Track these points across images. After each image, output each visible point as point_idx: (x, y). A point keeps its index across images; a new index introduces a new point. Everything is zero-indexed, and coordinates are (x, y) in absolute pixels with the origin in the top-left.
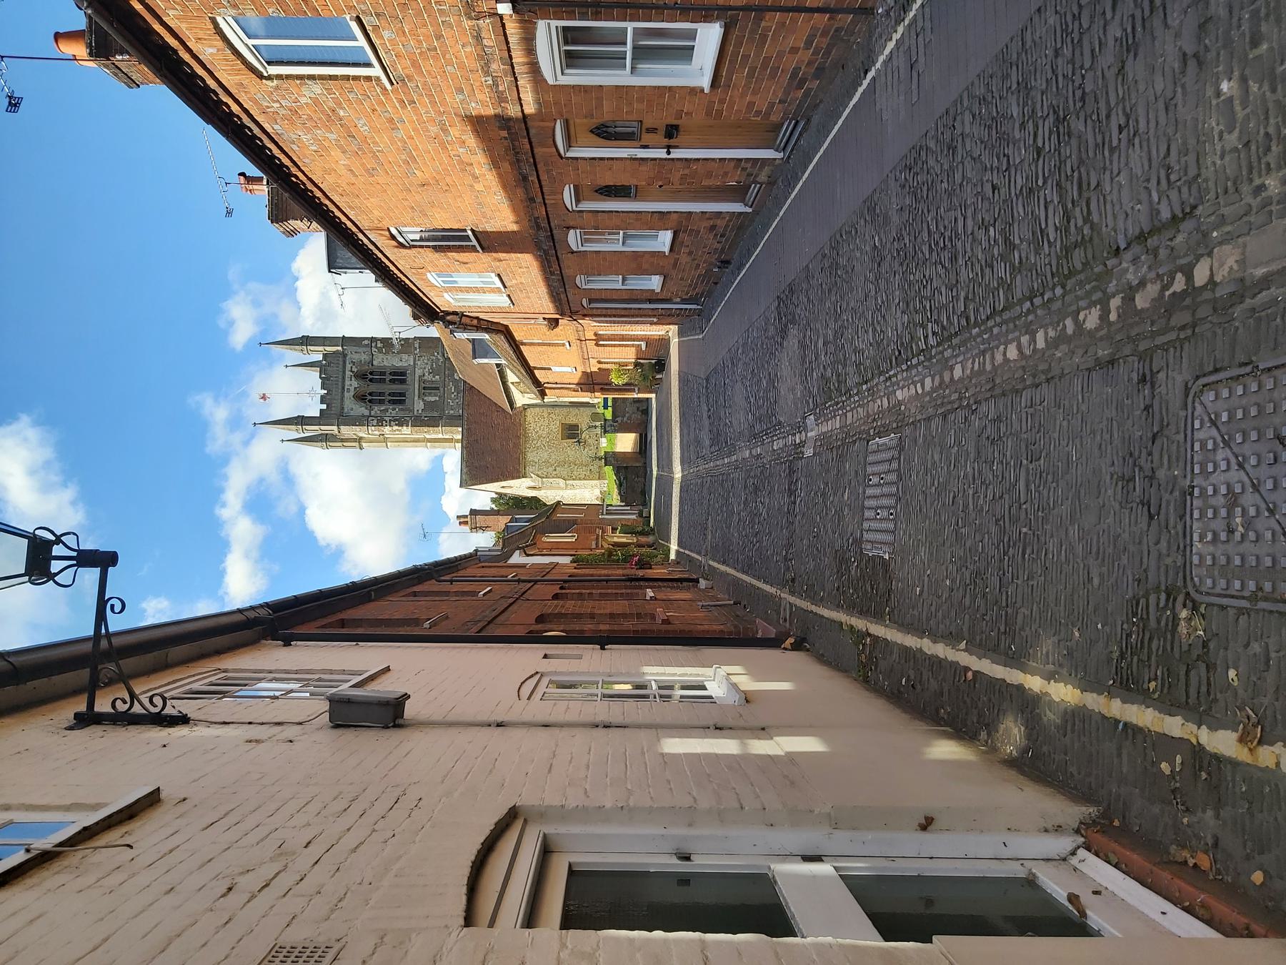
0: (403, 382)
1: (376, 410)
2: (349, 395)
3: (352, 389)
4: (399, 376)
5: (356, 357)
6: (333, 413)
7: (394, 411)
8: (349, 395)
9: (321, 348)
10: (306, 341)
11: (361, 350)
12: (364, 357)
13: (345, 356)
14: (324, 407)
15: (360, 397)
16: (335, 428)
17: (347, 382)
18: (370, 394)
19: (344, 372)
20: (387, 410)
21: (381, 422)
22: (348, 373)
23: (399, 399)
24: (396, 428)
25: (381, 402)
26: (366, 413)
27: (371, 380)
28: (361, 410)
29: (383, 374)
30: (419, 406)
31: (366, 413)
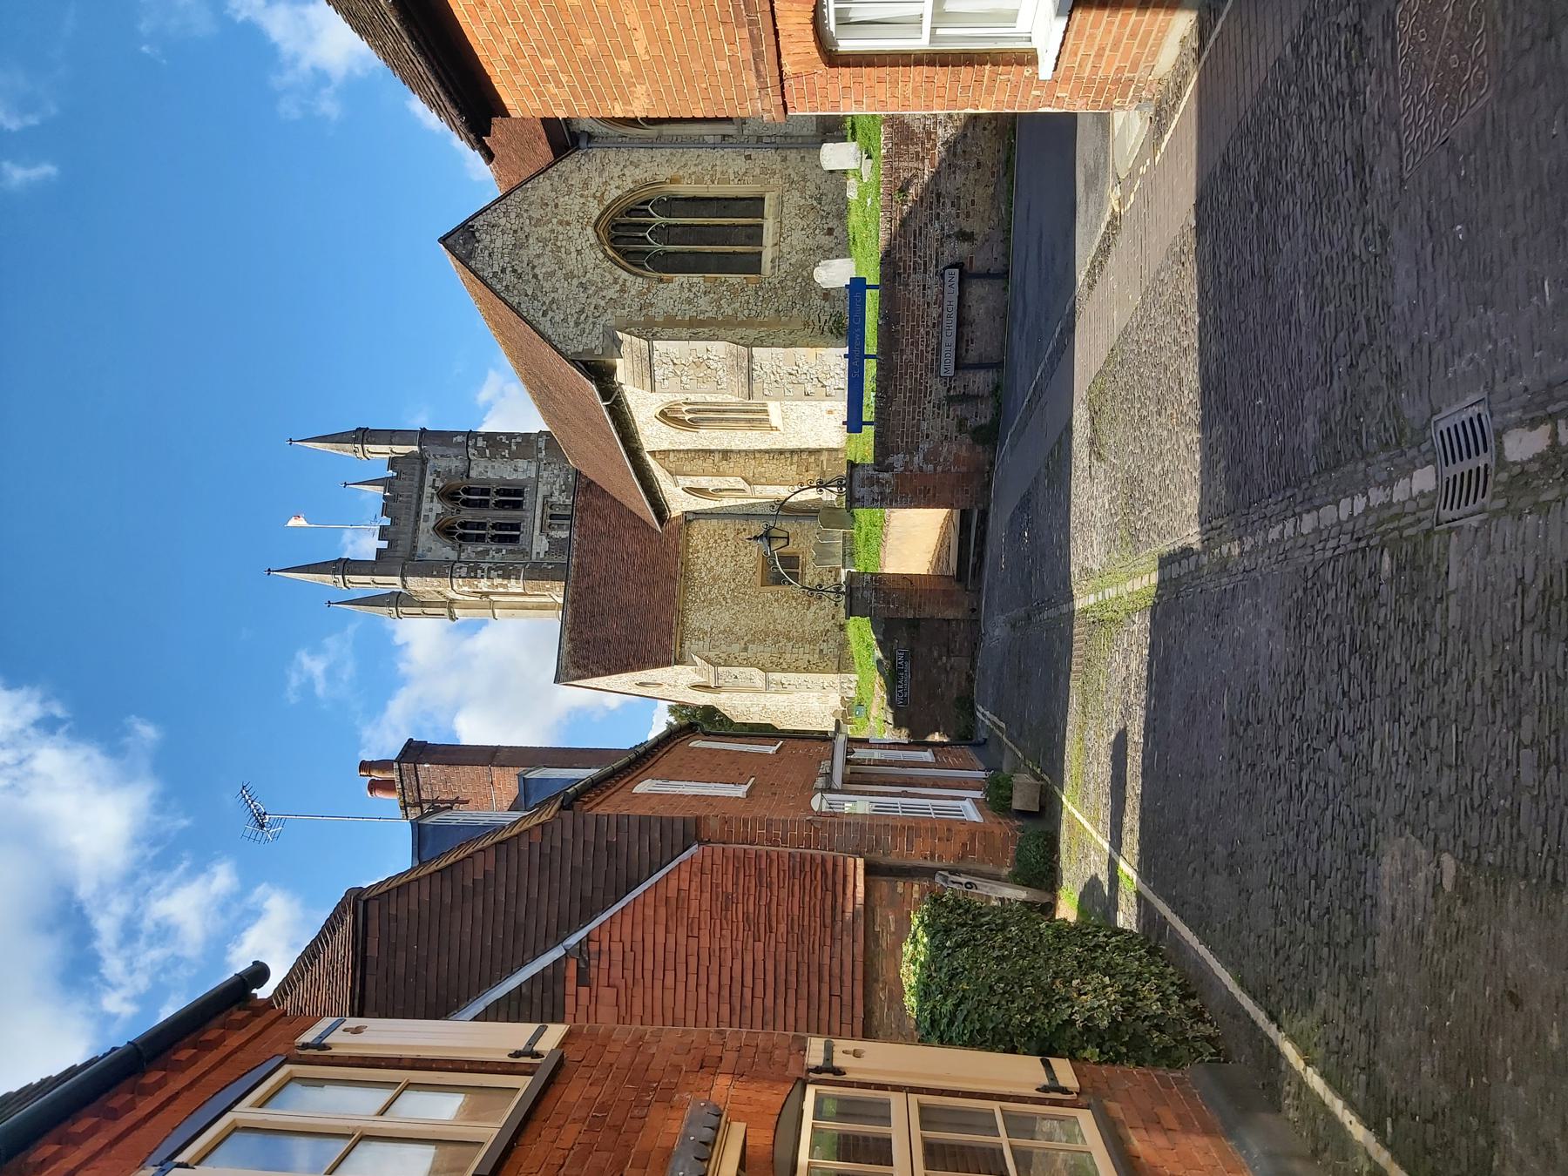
0: (518, 505)
1: (470, 550)
2: (426, 526)
3: (432, 516)
4: (512, 497)
5: (443, 464)
6: (397, 556)
7: (498, 553)
8: (426, 526)
9: (385, 448)
10: (363, 436)
11: (450, 452)
12: (456, 464)
13: (424, 462)
14: (384, 545)
15: (445, 530)
16: (397, 580)
17: (426, 505)
18: (464, 525)
19: (421, 488)
21: (473, 572)
22: (428, 490)
23: (508, 535)
24: (497, 581)
25: (480, 538)
26: (453, 555)
27: (466, 503)
28: (445, 551)
29: (486, 492)
30: (540, 545)
31: (453, 555)
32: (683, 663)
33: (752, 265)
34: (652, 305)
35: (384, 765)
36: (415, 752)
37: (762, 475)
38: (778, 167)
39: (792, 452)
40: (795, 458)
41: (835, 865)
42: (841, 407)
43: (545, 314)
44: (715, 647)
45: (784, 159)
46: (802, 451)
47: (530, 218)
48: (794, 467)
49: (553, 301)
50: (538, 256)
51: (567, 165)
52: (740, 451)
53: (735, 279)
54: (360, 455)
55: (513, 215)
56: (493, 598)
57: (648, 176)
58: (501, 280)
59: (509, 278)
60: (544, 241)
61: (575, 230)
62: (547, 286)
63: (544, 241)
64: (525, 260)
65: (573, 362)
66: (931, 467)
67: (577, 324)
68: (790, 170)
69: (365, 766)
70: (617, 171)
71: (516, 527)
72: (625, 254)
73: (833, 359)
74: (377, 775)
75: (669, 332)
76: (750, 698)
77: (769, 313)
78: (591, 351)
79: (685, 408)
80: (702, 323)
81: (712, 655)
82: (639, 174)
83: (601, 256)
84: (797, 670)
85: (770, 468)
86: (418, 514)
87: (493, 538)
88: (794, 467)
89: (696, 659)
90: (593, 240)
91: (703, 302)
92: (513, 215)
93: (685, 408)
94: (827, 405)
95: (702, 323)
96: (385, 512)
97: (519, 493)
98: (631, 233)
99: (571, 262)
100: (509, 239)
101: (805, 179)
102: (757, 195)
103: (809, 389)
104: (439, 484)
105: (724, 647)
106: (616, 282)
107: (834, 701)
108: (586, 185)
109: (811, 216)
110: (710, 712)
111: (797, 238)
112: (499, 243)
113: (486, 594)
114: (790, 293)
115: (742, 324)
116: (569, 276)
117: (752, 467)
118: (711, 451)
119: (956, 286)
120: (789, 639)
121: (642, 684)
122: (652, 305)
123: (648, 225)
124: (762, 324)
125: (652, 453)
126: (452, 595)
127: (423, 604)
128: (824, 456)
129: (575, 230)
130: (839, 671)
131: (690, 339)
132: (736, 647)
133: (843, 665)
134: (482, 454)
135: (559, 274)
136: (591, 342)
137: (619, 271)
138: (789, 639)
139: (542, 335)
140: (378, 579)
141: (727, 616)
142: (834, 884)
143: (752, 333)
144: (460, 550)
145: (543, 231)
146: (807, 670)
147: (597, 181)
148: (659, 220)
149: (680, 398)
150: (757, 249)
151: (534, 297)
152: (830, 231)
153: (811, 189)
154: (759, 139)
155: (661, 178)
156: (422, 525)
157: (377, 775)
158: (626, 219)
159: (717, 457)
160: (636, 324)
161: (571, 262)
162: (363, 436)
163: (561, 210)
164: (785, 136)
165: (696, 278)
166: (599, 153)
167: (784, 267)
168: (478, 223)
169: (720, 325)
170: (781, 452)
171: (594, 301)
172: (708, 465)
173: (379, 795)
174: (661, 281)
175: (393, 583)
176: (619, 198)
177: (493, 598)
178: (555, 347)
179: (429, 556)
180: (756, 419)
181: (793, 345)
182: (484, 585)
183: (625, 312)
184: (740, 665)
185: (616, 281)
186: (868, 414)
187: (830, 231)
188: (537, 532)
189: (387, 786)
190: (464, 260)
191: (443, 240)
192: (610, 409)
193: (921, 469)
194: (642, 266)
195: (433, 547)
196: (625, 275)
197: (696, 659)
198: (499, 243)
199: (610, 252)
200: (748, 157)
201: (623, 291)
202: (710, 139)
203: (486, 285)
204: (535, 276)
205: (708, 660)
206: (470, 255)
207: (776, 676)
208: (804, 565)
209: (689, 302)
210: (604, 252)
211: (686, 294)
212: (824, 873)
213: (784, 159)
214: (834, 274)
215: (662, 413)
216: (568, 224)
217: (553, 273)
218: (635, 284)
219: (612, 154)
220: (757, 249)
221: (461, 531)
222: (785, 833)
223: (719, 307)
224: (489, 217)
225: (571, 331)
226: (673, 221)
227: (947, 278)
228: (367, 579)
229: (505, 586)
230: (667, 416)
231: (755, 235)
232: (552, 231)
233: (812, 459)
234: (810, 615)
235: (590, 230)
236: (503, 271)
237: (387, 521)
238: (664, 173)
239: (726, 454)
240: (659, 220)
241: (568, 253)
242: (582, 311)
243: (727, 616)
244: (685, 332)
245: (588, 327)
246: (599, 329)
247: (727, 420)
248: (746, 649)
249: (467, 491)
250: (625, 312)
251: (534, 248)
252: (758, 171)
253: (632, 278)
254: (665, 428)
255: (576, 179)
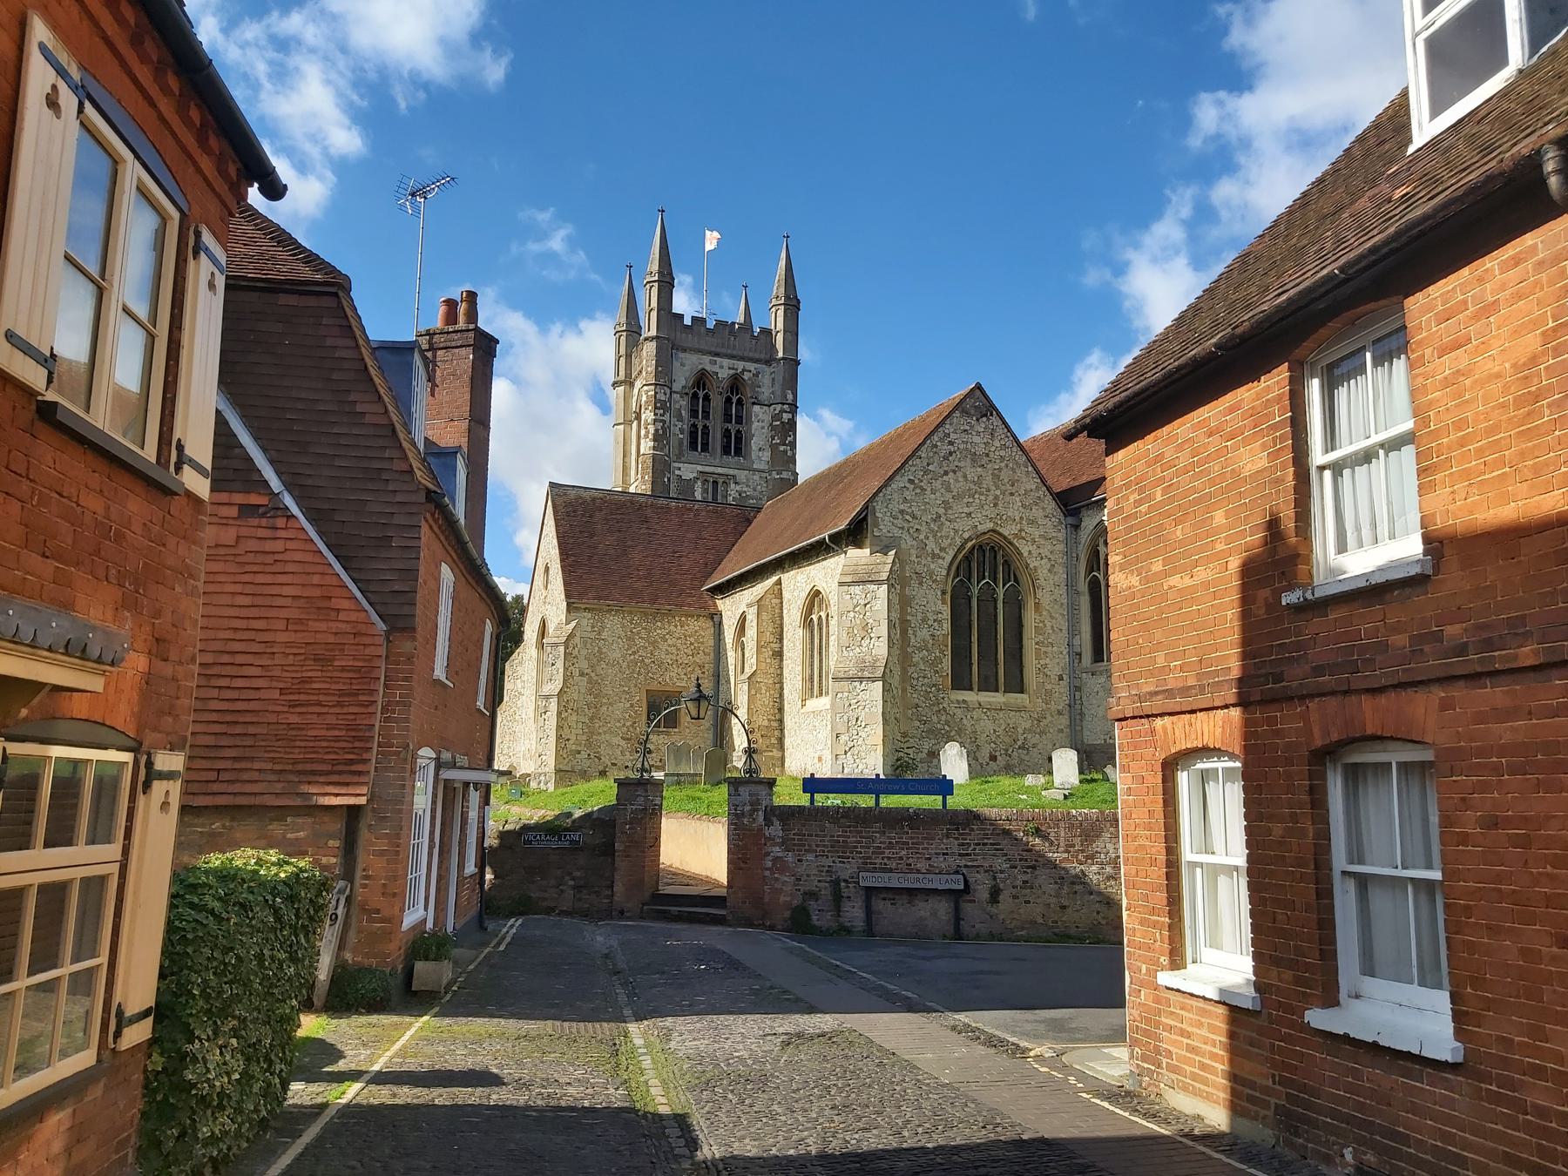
0: (726, 450)
1: (683, 403)
2: (705, 362)
3: (716, 369)
4: (735, 445)
5: (765, 380)
6: (676, 335)
7: (679, 430)
8: (705, 362)
9: (780, 326)
10: (792, 306)
11: (777, 387)
12: (765, 392)
13: (768, 362)
14: (687, 321)
15: (702, 380)
16: (653, 332)
17: (726, 362)
18: (707, 398)
19: (742, 359)
20: (680, 419)
21: (660, 406)
22: (740, 365)
23: (697, 441)
24: (652, 429)
25: (694, 413)
27: (728, 400)
28: (682, 379)
29: (739, 420)
30: (687, 471)
31: (677, 387)
32: (568, 611)
33: (960, 681)
34: (921, 584)
35: (472, 315)
36: (485, 347)
37: (758, 691)
38: (1053, 707)
39: (781, 721)
40: (775, 724)
41: (360, 773)
42: (825, 771)
43: (911, 481)
44: (585, 643)
45: (1060, 713)
46: (782, 730)
47: (1000, 469)
48: (766, 723)
49: (923, 490)
50: (965, 476)
51: (1050, 505)
52: (781, 668)
53: (947, 664)
54: (774, 302)
55: (1003, 453)
56: (635, 424)
57: (1042, 582)
58: (941, 440)
59: (945, 448)
60: (978, 483)
61: (989, 511)
62: (937, 484)
63: (978, 483)
64: (962, 464)
65: (866, 507)
66: (769, 864)
67: (902, 512)
68: (1049, 718)
69: (472, 297)
70: (1045, 552)
71: (705, 448)
72: (967, 558)
73: (871, 763)
74: (462, 309)
75: (896, 600)
76: (530, 682)
77: (915, 698)
78: (876, 525)
79: (823, 614)
80: (904, 632)
81: (577, 640)
82: (1043, 573)
83: (966, 536)
84: (559, 727)
85: (765, 699)
86: (717, 355)
87: (694, 426)
88: (766, 723)
89: (573, 624)
90: (981, 528)
91: (924, 633)
92: (1003, 453)
93: (823, 614)
94: (827, 756)
95: (904, 632)
96: (719, 323)
97: (738, 452)
98: (986, 569)
99: (960, 508)
100: (980, 450)
101: (1042, 733)
102: (1026, 686)
103: (843, 738)
104: (746, 376)
105: (584, 652)
106: (942, 549)
107: (525, 767)
108: (1032, 522)
109: (1007, 739)
110: (517, 639)
111: (986, 726)
112: (977, 439)
113: (638, 417)
114: (935, 718)
115: (904, 671)
116: (947, 505)
117: (766, 680)
118: (781, 640)
119: (947, 886)
120: (591, 719)
121: (547, 569)
122: (921, 584)
123: (995, 580)
124: (904, 690)
125: (779, 582)
126: (638, 384)
127: (629, 356)
128: (776, 754)
129: (989, 511)
130: (558, 771)
131: (890, 621)
132: (584, 665)
133: (565, 775)
134: (776, 417)
135: (948, 496)
136: (884, 523)
137: (952, 553)
138: (591, 719)
139: (891, 478)
140: (654, 314)
141: (617, 655)
142: (340, 773)
143: (895, 681)
144: (683, 394)
145: (988, 481)
146: (559, 737)
147: (1036, 532)
148: (1001, 592)
149: (833, 610)
150: (975, 687)
151: (926, 472)
152: (993, 758)
153: (1035, 739)
154: (1078, 689)
155: (1039, 594)
156: (707, 358)
157: (462, 309)
158: (1000, 560)
159: (776, 646)
160: (902, 567)
161: (960, 508)
162: (792, 306)
163: (1008, 498)
164: (1082, 714)
165: (947, 626)
166: (1061, 535)
167: (958, 712)
168: (994, 419)
169: (903, 650)
170: (781, 710)
171: (923, 528)
172: (768, 637)
173: (442, 310)
174: (944, 593)
175: (650, 327)
176: (1020, 554)
177: (635, 424)
178: (879, 490)
179: (676, 364)
180: (814, 686)
181: (885, 721)
182: (648, 415)
183: (913, 558)
184: (566, 669)
185: (942, 549)
186: (820, 799)
187: (993, 758)
188: (700, 468)
189: (451, 317)
190: (960, 406)
191: (979, 387)
192: (821, 543)
193: (768, 854)
194: (957, 575)
195: (686, 367)
196: (949, 558)
197: (573, 624)
198: (977, 439)
199: (969, 545)
200: (1061, 678)
201: (934, 556)
202: (1076, 641)
203: (938, 427)
204: (946, 473)
205: (571, 636)
206: (965, 412)
207: (553, 706)
208: (668, 734)
209: (924, 620)
210: (970, 539)
211: (931, 617)
212: (351, 762)
213: (1060, 713)
214: (954, 764)
215: (818, 593)
216: (995, 505)
217: (949, 490)
218: (940, 568)
219: (1061, 547)
220: (975, 687)
221: (701, 394)
222: (396, 720)
223: (920, 649)
224: (1001, 430)
225: (895, 506)
226: (1000, 605)
227: (953, 877)
228: (654, 304)
229: (646, 436)
230: (815, 597)
231: (988, 685)
232: (988, 490)
233: (773, 741)
234: (616, 740)
235: (990, 525)
236: (951, 443)
237: (711, 324)
238: (1045, 598)
239: (779, 654)
240: (1001, 592)
241: (968, 505)
242: (914, 517)
243: (617, 655)
244: (896, 616)
245: (899, 522)
246: (897, 533)
247: (812, 656)
248: (582, 674)
249: (740, 402)
250: (913, 558)
251: (972, 473)
252: (1049, 687)
253: (946, 565)
254: (804, 595)
255: (1037, 513)
